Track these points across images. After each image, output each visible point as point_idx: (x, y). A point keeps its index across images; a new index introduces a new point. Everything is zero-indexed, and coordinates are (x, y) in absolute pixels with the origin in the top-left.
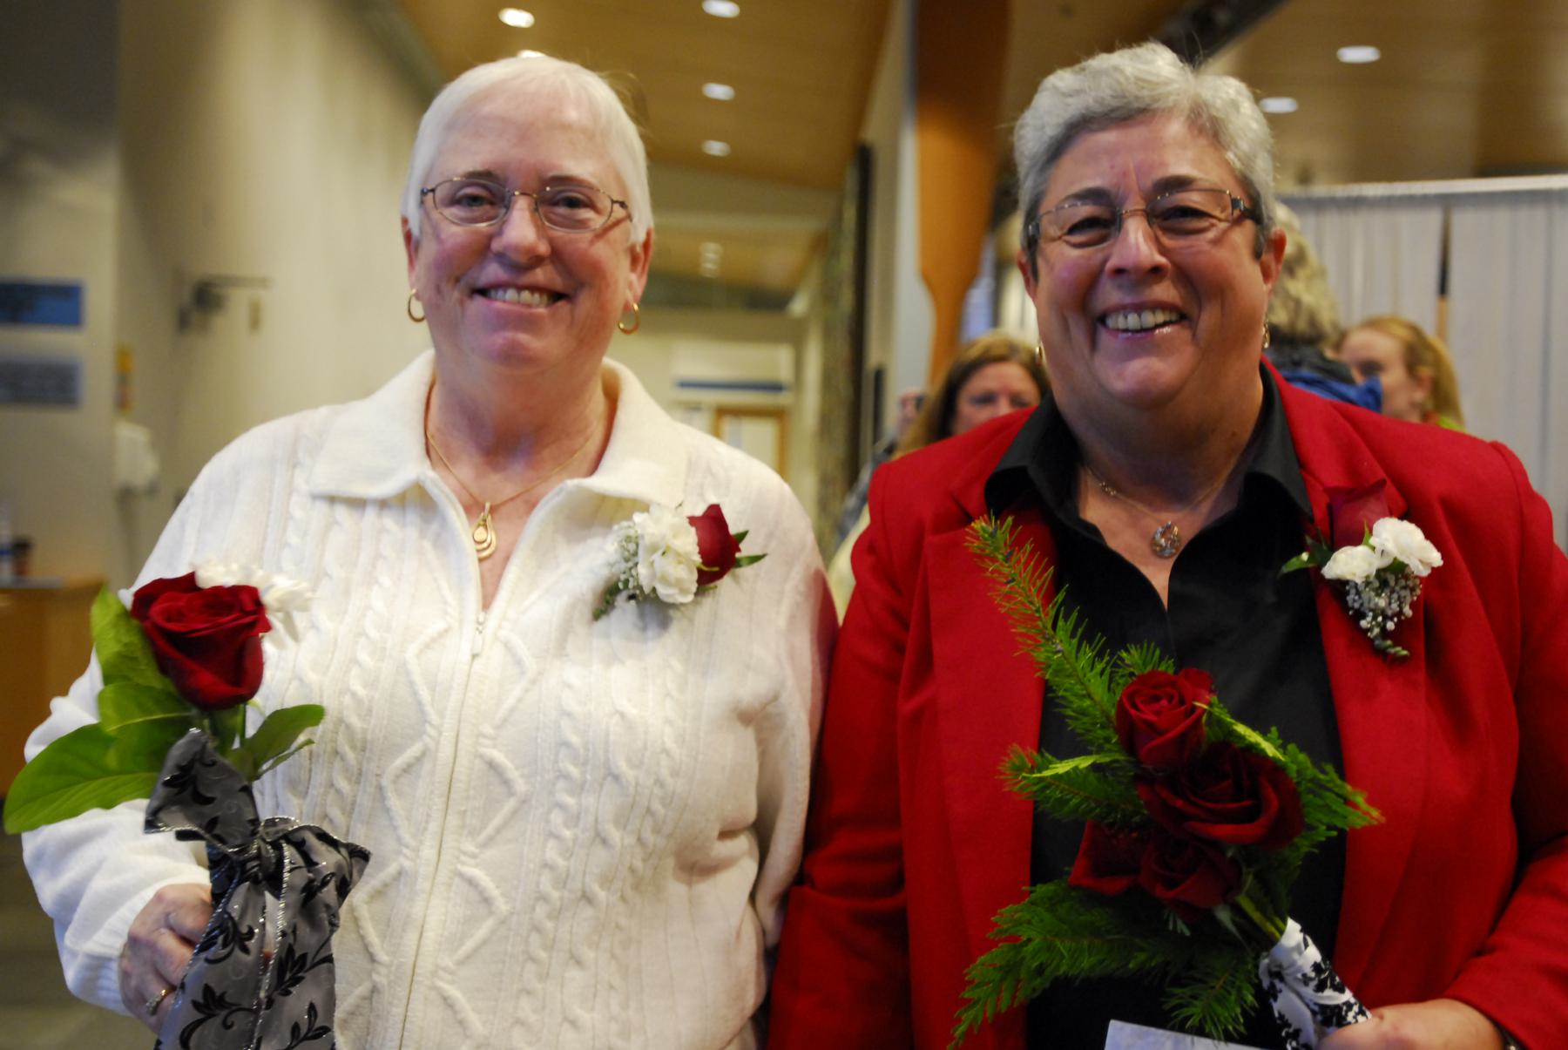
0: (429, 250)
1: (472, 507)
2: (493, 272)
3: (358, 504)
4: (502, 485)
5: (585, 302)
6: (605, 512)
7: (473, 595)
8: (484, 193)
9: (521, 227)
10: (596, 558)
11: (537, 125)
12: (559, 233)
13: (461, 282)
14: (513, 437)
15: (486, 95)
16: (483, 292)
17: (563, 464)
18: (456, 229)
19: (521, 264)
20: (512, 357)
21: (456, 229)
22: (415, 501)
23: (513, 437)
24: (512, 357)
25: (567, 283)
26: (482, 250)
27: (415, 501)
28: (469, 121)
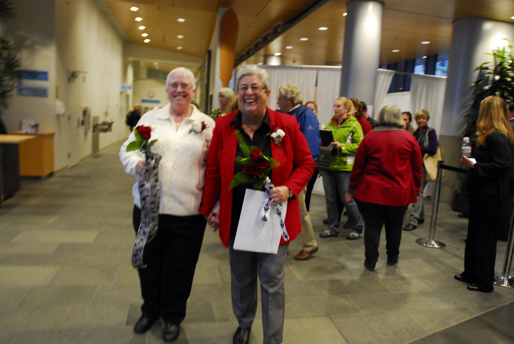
0: (169, 92)
1: (175, 120)
2: (176, 94)
3: (162, 120)
4: (179, 118)
5: (188, 97)
6: (190, 122)
7: (175, 130)
8: (175, 85)
9: (179, 89)
10: (189, 127)
11: (182, 77)
12: (184, 90)
13: (173, 95)
14: (179, 113)
15: (175, 73)
16: (175, 96)
17: (186, 116)
18: (172, 89)
19: (180, 93)
20: (179, 104)
21: (172, 89)
22: (168, 120)
23: (179, 113)
24: (179, 104)
25: (185, 95)
26: (175, 91)
27: (168, 120)
28: (173, 76)
